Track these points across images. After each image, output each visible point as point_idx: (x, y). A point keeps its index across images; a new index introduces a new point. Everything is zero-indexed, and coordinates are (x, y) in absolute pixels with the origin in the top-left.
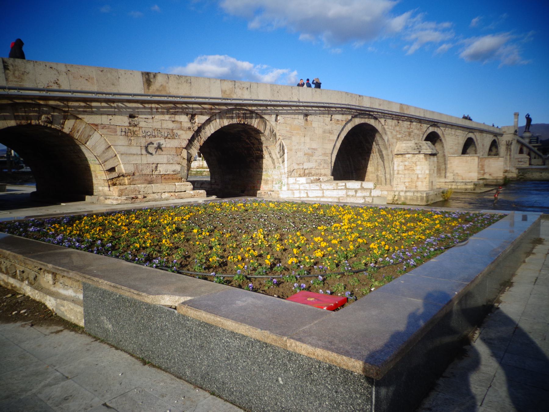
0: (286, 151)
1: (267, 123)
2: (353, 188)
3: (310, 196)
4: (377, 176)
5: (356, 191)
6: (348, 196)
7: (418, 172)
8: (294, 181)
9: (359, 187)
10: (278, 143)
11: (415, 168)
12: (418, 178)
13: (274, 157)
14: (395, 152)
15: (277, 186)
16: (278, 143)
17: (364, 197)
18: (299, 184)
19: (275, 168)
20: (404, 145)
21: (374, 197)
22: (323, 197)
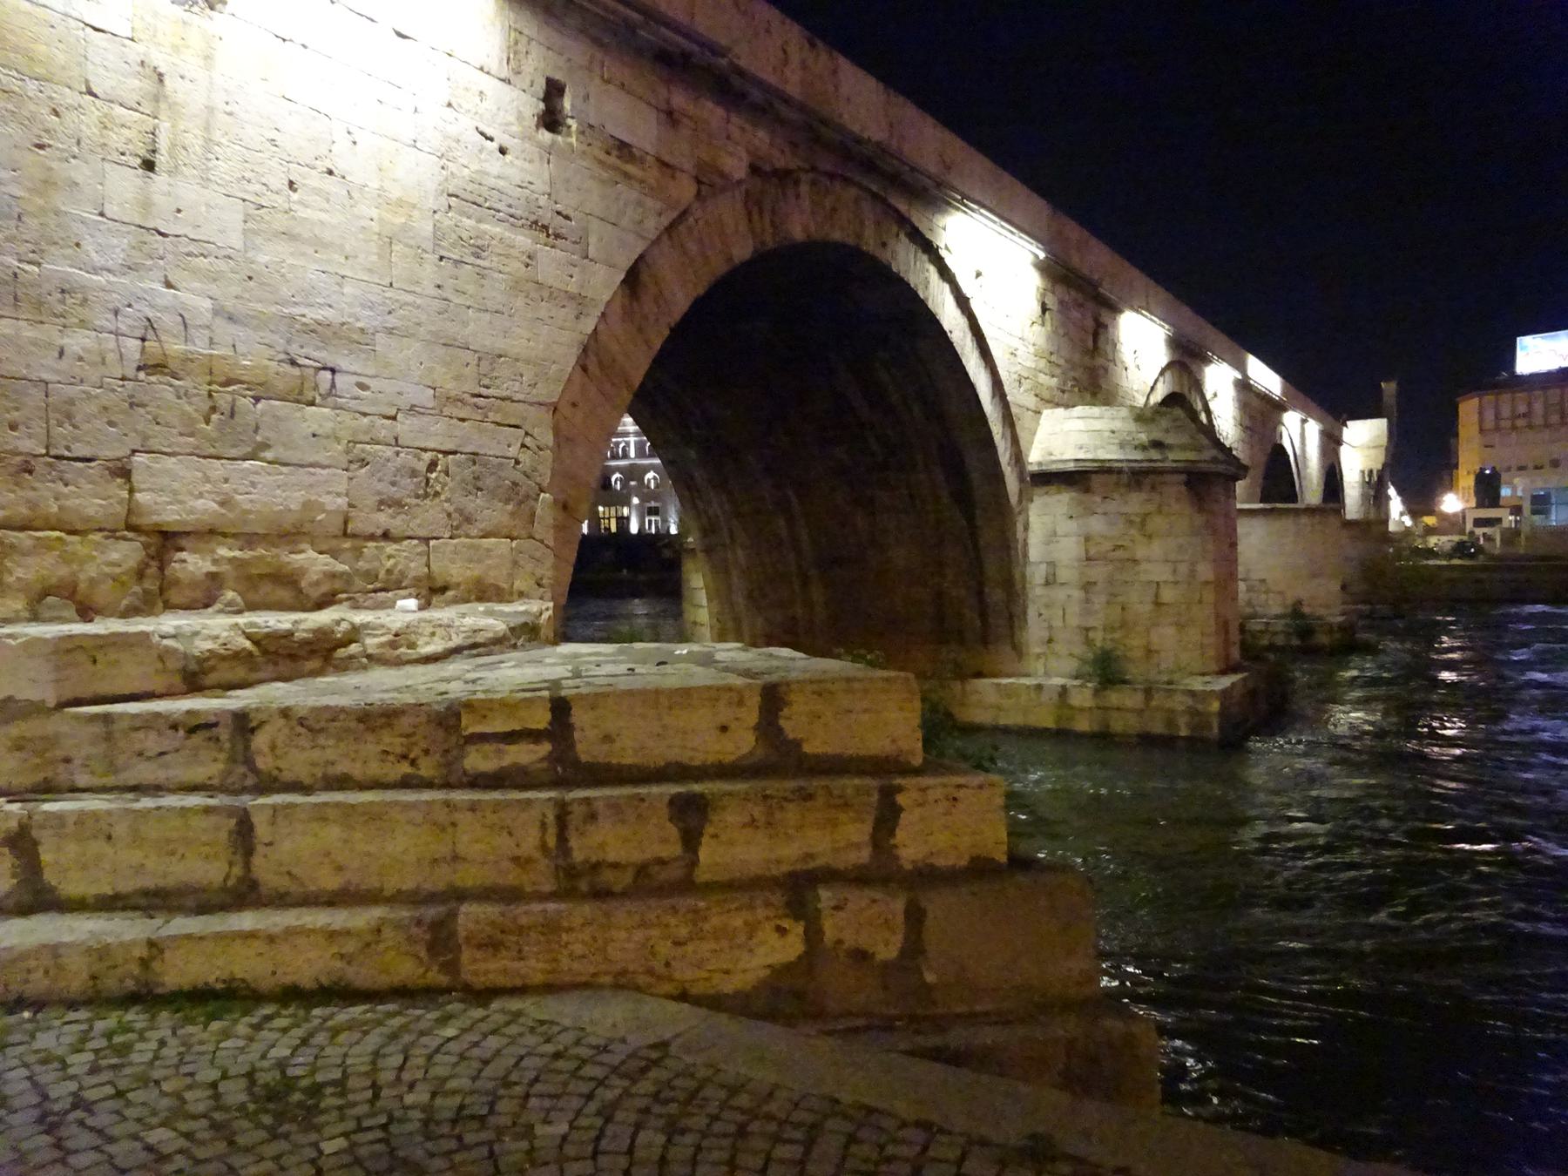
3: (73, 886)
4: (939, 595)
5: (691, 816)
7: (1160, 573)
9: (743, 743)
11: (1140, 552)
12: (1158, 604)
14: (1035, 468)
17: (797, 890)
20: (1080, 424)
21: (928, 877)
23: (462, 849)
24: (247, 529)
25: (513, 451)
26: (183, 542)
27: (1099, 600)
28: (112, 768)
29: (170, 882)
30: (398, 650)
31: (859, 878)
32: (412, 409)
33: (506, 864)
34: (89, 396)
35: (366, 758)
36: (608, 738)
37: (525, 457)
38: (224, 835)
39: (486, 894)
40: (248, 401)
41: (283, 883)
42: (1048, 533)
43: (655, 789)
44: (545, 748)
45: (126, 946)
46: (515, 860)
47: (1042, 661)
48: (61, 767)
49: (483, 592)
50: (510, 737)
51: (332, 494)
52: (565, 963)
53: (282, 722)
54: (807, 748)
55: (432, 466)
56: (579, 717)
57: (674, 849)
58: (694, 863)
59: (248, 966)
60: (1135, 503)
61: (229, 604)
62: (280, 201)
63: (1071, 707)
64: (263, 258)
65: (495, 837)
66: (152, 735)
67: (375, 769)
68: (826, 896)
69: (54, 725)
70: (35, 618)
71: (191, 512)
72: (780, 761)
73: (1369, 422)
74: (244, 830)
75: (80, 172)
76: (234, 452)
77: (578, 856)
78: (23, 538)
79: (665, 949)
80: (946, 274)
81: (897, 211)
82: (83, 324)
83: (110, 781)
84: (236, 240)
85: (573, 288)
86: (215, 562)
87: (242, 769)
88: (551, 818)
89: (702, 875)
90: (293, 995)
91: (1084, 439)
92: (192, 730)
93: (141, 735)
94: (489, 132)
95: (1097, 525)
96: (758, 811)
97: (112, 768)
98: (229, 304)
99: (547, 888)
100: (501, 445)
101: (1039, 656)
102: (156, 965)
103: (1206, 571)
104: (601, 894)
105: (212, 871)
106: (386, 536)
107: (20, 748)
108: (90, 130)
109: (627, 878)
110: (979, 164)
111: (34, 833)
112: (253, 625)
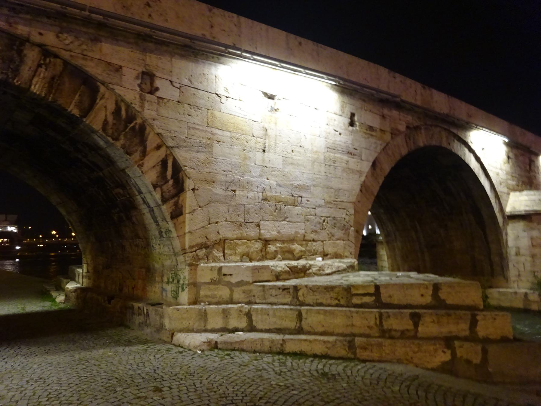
0: (189, 184)
1: (102, 89)
2: (404, 302)
3: (260, 326)
5: (416, 318)
6: (385, 333)
8: (215, 275)
9: (428, 299)
10: (153, 159)
13: (152, 205)
14: (509, 214)
16: (153, 159)
17: (448, 341)
18: (229, 284)
19: (160, 233)
20: (526, 198)
21: (486, 341)
22: (300, 331)
23: (354, 323)
24: (283, 239)
25: (344, 216)
26: (270, 243)
28: (265, 299)
29: (282, 327)
30: (320, 272)
31: (466, 339)
32: (320, 206)
33: (366, 328)
34: (252, 207)
35: (325, 298)
36: (390, 297)
37: (347, 218)
38: (295, 316)
39: (361, 335)
40: (283, 207)
41: (309, 329)
42: (515, 237)
43: (406, 311)
44: (373, 298)
45: (278, 340)
46: (368, 327)
47: (516, 283)
48: (253, 298)
49: (337, 256)
50: (364, 295)
51: (300, 229)
52: (384, 354)
53: (305, 288)
54: (448, 302)
55: (324, 221)
56: (382, 290)
57: (411, 327)
58: (417, 331)
59: (305, 348)
61: (279, 258)
62: (290, 155)
63: (529, 300)
64: (287, 170)
65: (364, 320)
66: (274, 291)
67: (329, 301)
68: (457, 343)
69: (252, 287)
70: (242, 261)
71: (272, 235)
72: (438, 305)
74: (300, 316)
75: (251, 155)
76: (280, 219)
77: (385, 327)
78: (239, 242)
79: (411, 354)
80: (471, 151)
81: (454, 133)
82: (251, 190)
83: (264, 301)
84: (281, 167)
85: (358, 169)
86: (276, 248)
87: (296, 300)
88: (377, 316)
89: (419, 335)
90: (315, 356)
91: (529, 203)
92: (284, 290)
93: (271, 290)
94: (336, 130)
95: (535, 233)
96: (435, 318)
97: (265, 299)
98: (280, 182)
99: (377, 335)
100: (341, 214)
101: (514, 282)
102: (284, 346)
104: (392, 338)
105: (292, 324)
106: (314, 240)
107: (244, 293)
108: (253, 145)
109: (399, 334)
110: (481, 113)
111: (252, 313)
112: (289, 264)
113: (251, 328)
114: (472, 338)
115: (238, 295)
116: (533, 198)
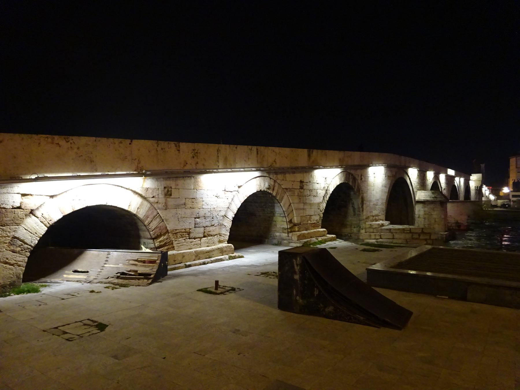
5: (419, 235)
6: (413, 239)
7: (435, 216)
11: (433, 213)
12: (435, 221)
15: (355, 229)
17: (426, 240)
18: (374, 229)
19: (355, 215)
20: (423, 194)
21: (433, 240)
22: (393, 239)
27: (427, 220)
35: (398, 232)
42: (419, 210)
59: (397, 242)
60: (432, 206)
65: (408, 236)
73: (477, 175)
80: (408, 176)
95: (426, 209)
103: (443, 216)
105: (391, 237)
113: (381, 238)
114: (430, 239)
115: (375, 231)
116: (427, 194)
